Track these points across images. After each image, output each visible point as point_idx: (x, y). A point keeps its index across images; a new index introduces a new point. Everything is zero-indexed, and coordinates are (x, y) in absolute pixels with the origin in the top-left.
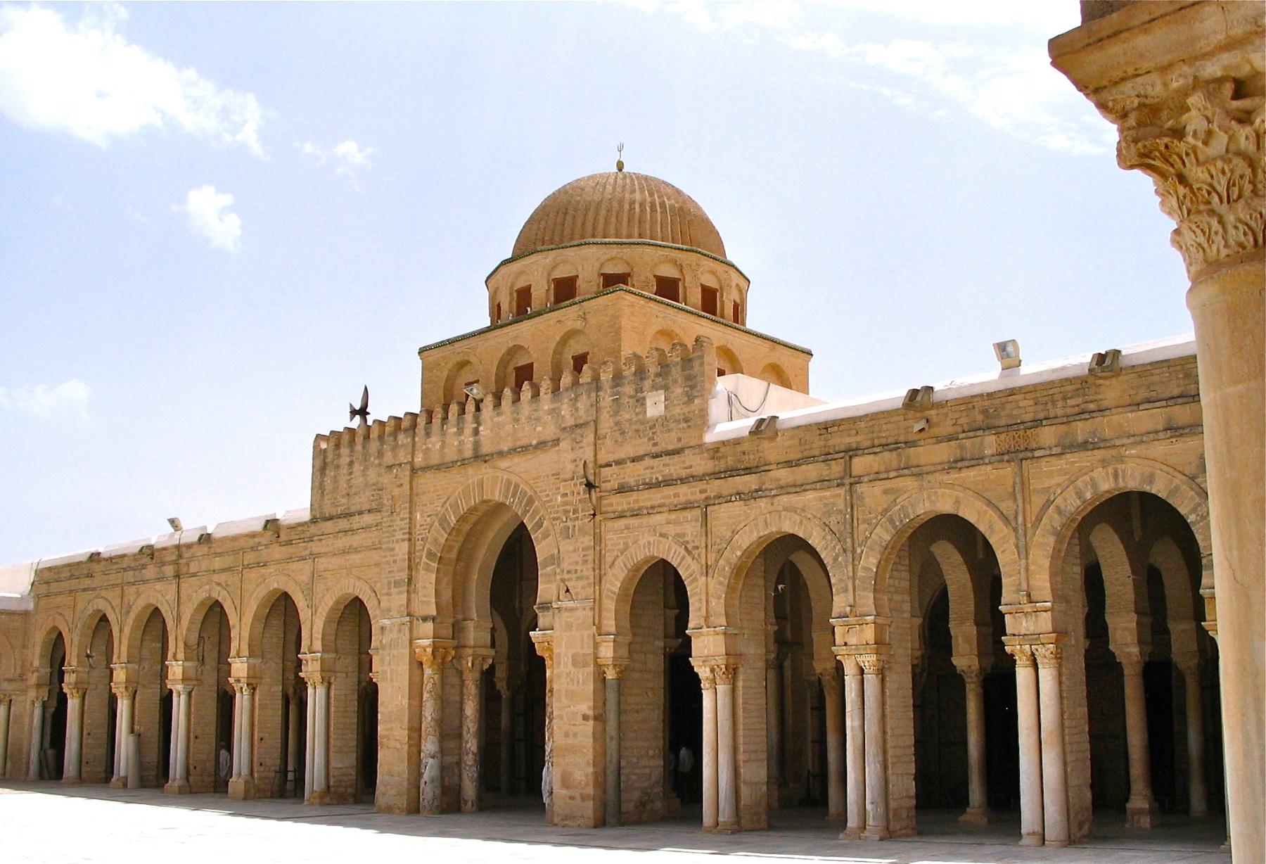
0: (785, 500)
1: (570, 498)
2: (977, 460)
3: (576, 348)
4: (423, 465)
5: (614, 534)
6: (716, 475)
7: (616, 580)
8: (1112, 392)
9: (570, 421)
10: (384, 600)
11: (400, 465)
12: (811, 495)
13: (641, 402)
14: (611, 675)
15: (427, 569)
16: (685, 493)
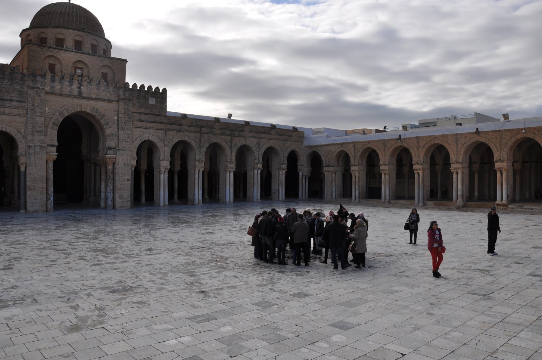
0: (186, 133)
1: (123, 119)
2: (225, 135)
3: (105, 70)
4: (50, 91)
5: (137, 132)
6: (170, 124)
7: (137, 144)
8: (246, 128)
9: (122, 96)
10: (29, 137)
11: (38, 88)
12: (192, 134)
14: (133, 169)
15: (52, 128)
16: (160, 126)
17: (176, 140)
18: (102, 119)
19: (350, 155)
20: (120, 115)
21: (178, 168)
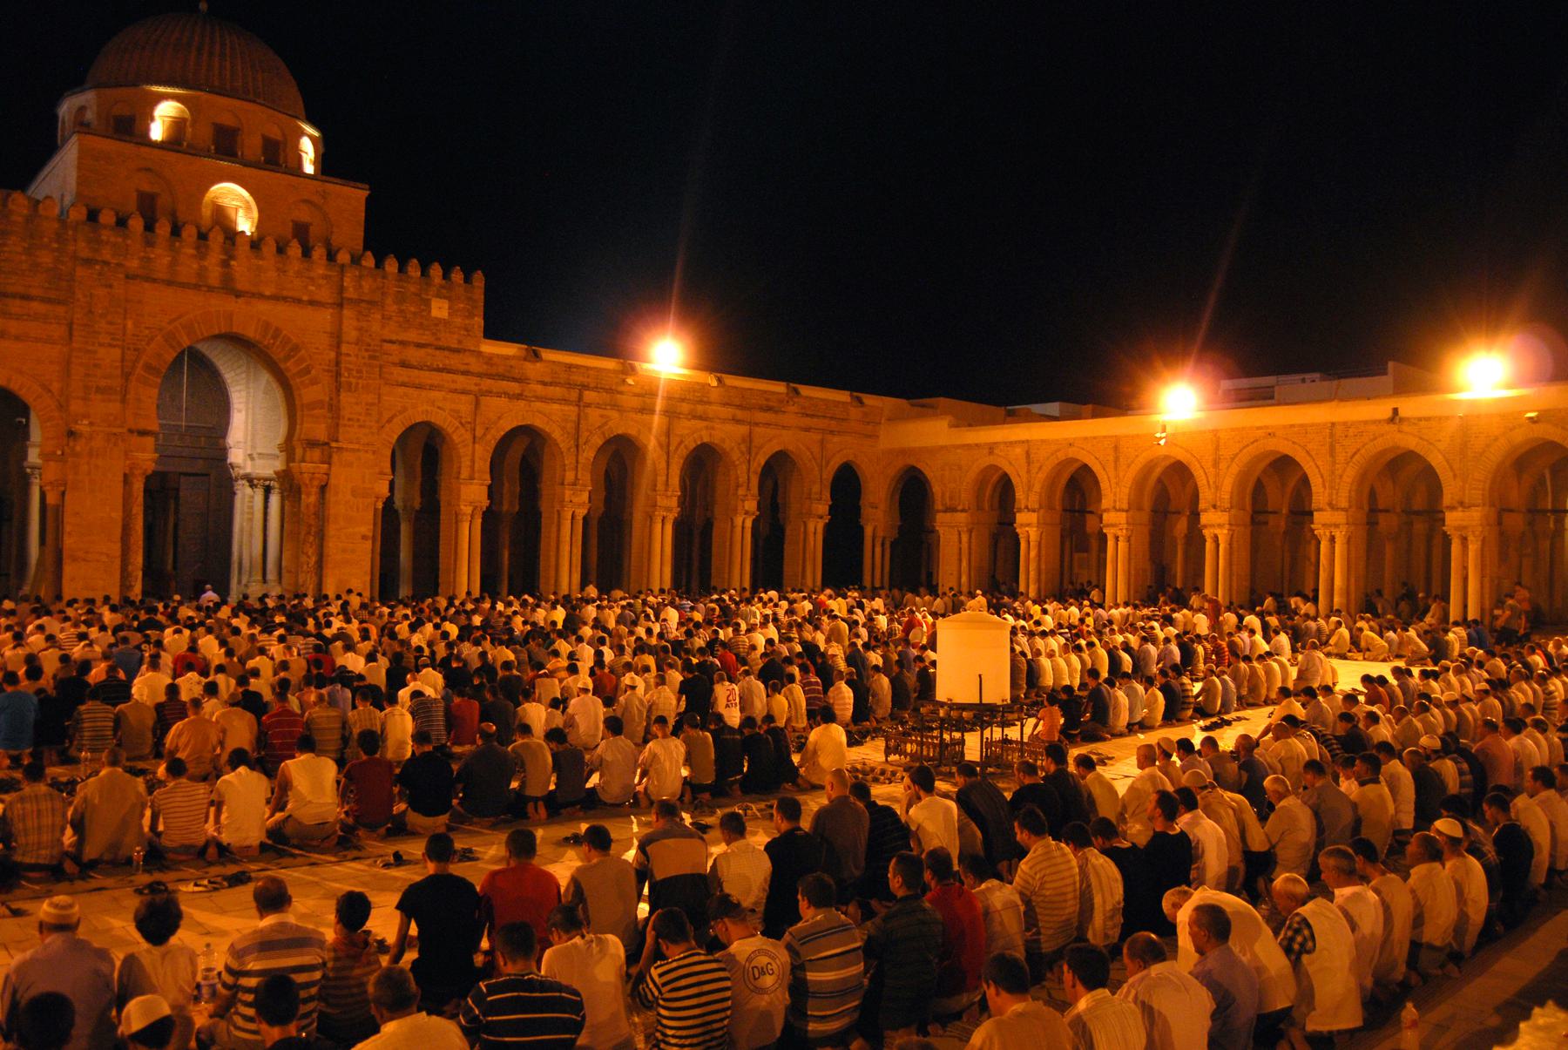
1: (353, 359)
3: (304, 215)
10: (76, 406)
11: (107, 263)
13: (427, 303)
14: (380, 505)
17: (507, 425)
18: (288, 357)
19: (1015, 480)
20: (344, 348)
21: (509, 505)
